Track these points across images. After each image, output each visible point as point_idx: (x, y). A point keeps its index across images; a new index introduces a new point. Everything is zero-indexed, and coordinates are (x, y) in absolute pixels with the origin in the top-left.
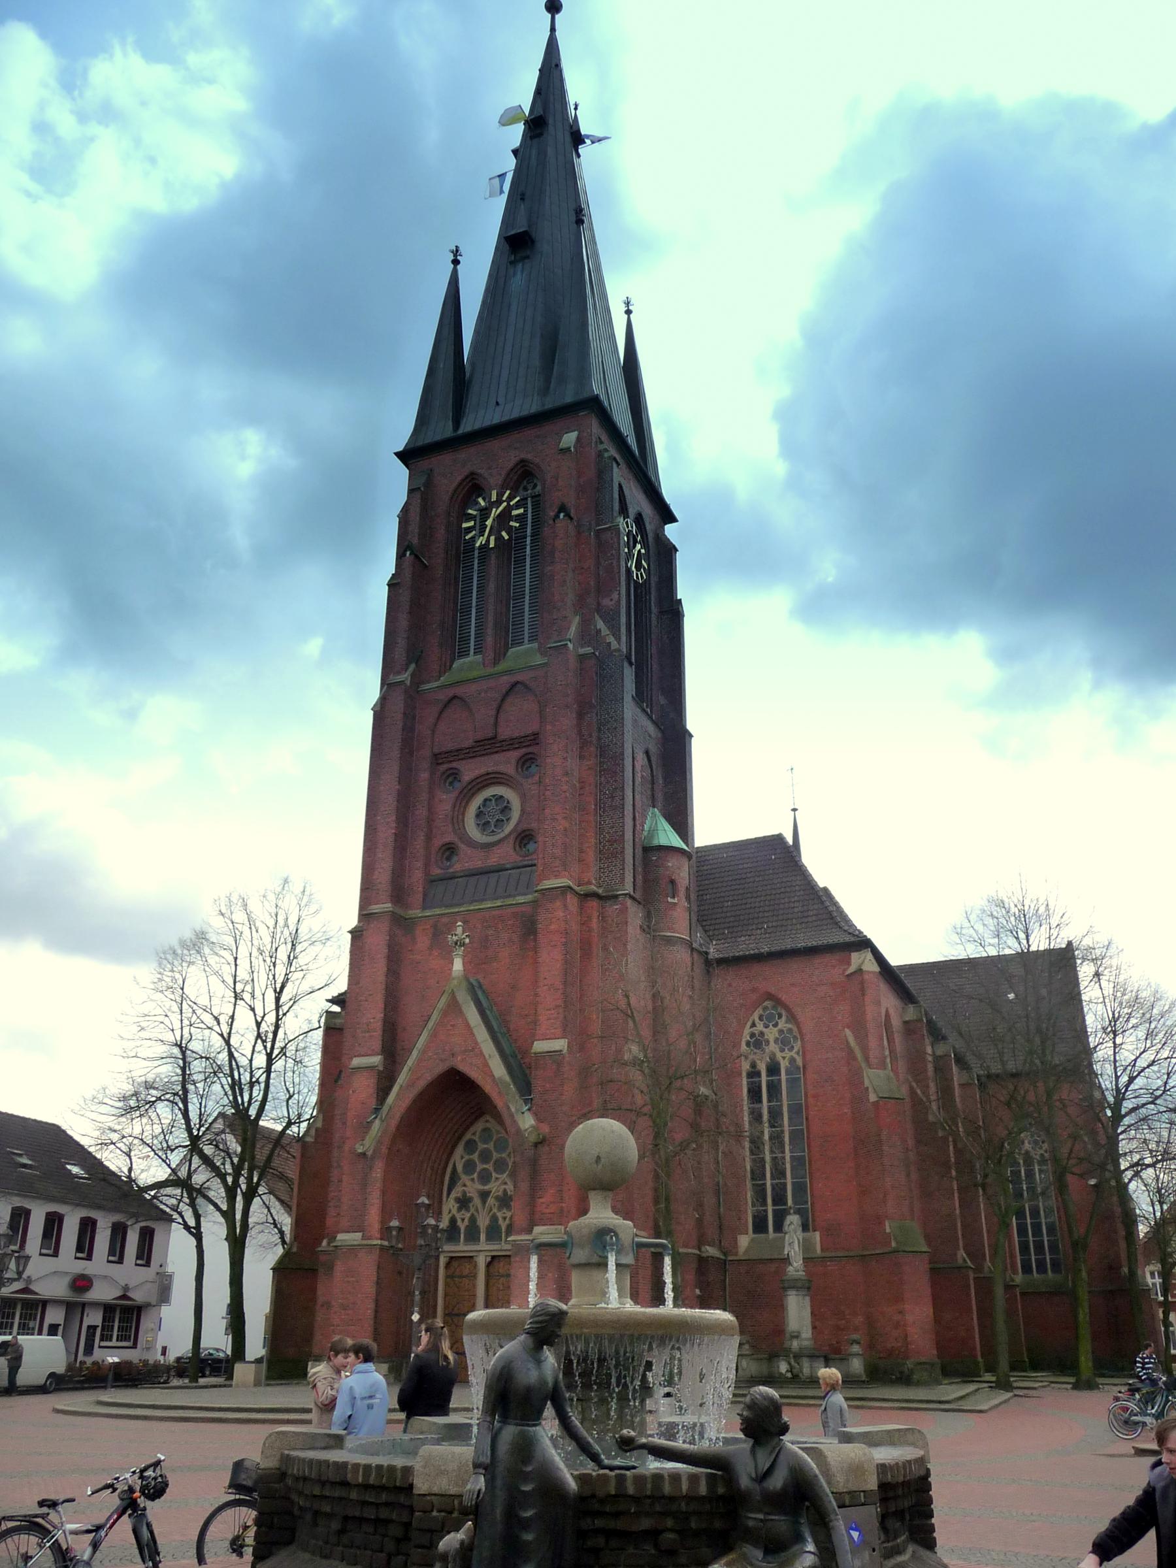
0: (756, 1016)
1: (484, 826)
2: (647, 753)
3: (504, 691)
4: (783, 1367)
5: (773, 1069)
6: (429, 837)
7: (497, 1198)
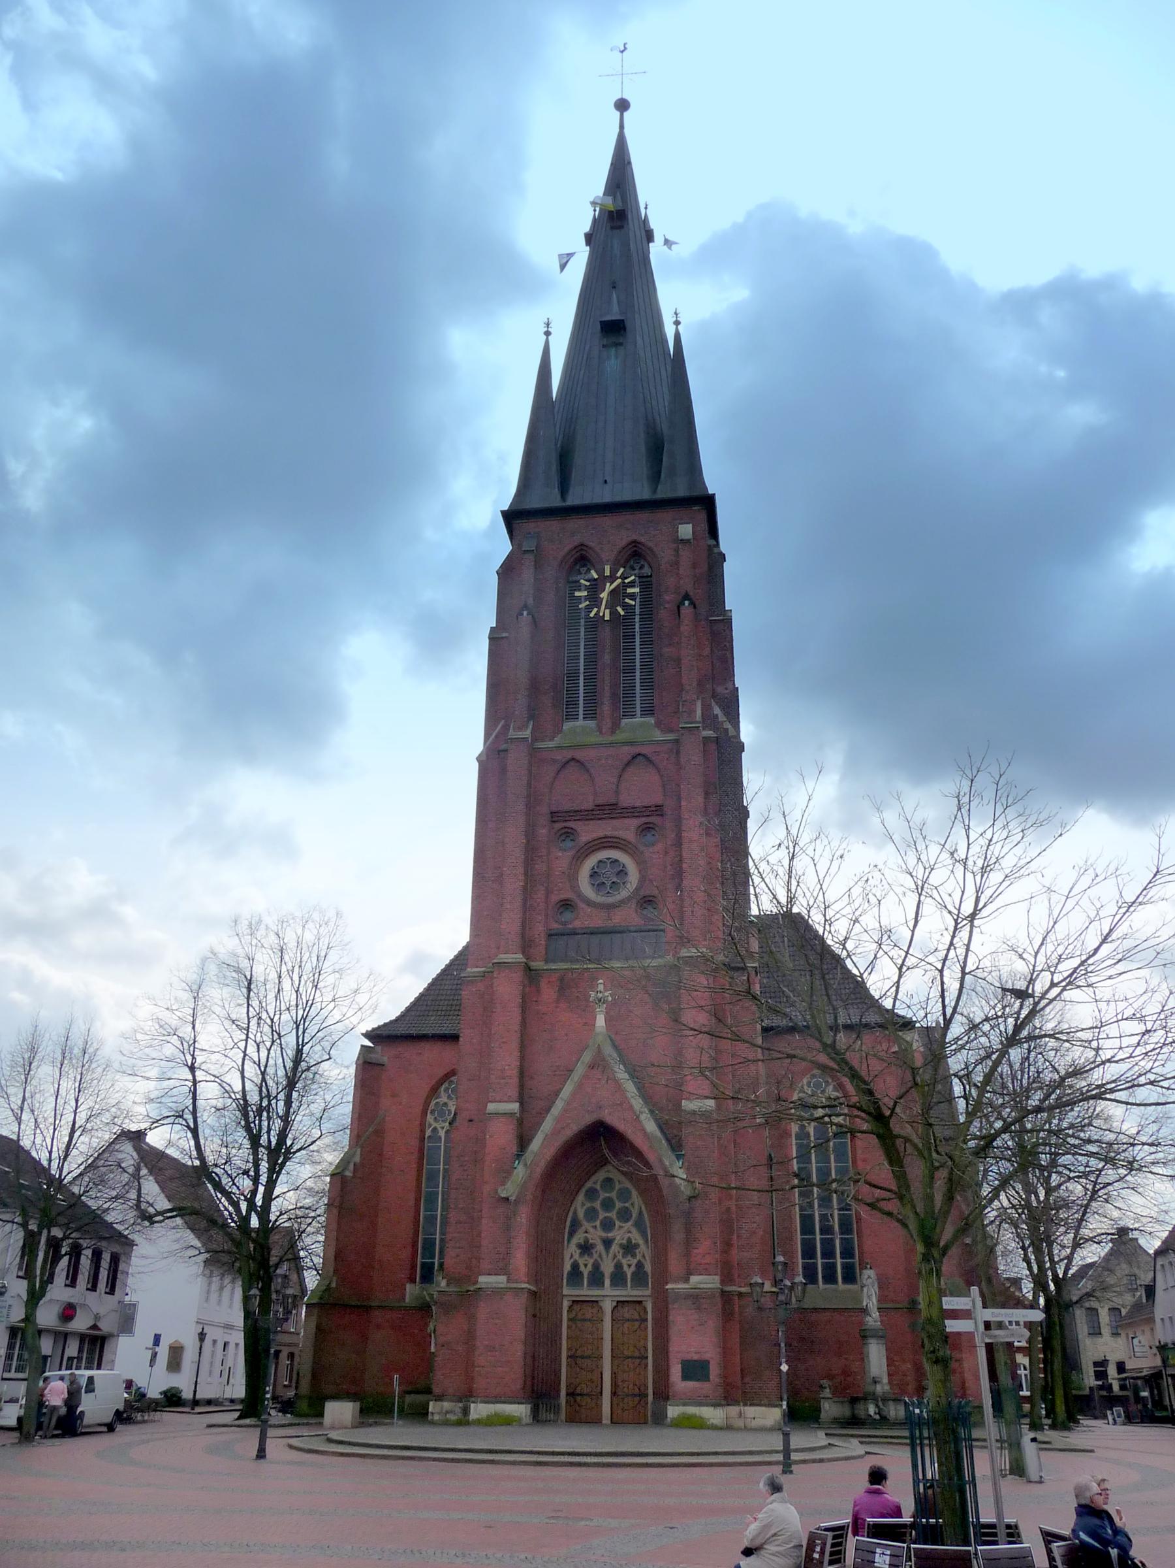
3: (625, 760)
6: (548, 893)
7: (621, 1246)
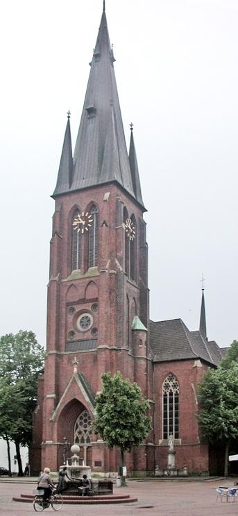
2: (134, 299)
4: (166, 473)
5: (171, 394)
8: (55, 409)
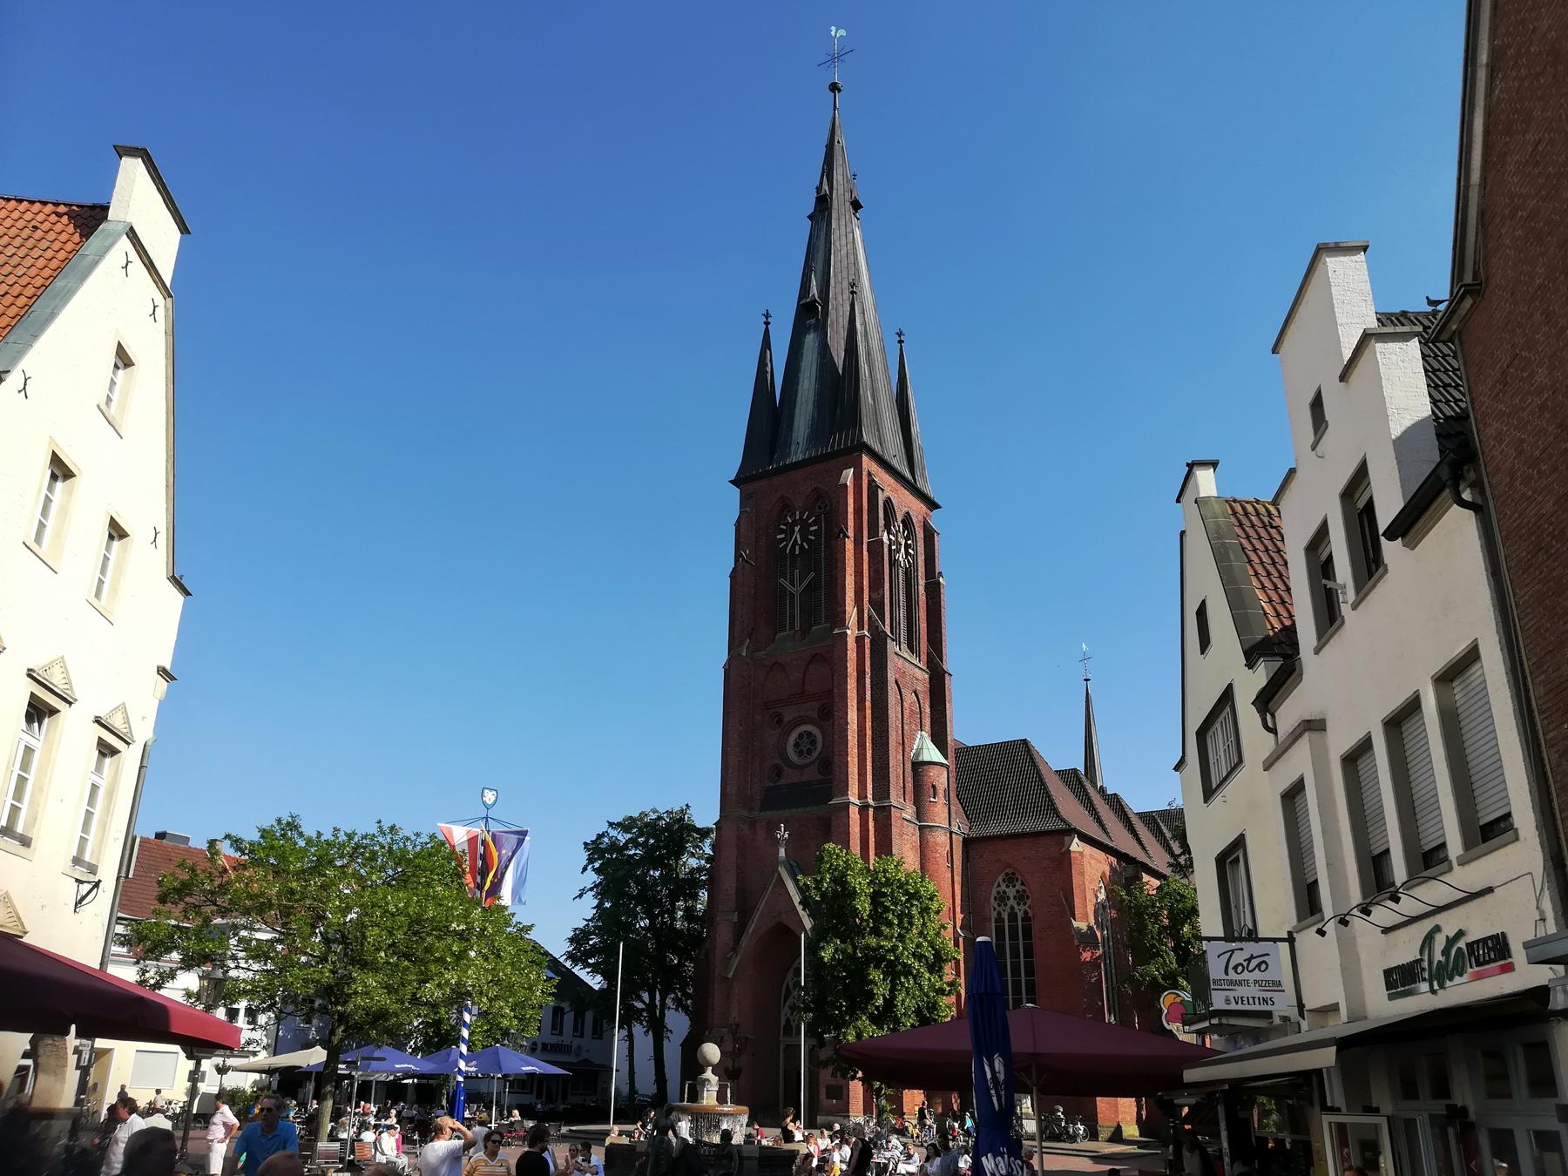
0: (1000, 879)
1: (800, 753)
5: (1013, 917)
8: (735, 949)
